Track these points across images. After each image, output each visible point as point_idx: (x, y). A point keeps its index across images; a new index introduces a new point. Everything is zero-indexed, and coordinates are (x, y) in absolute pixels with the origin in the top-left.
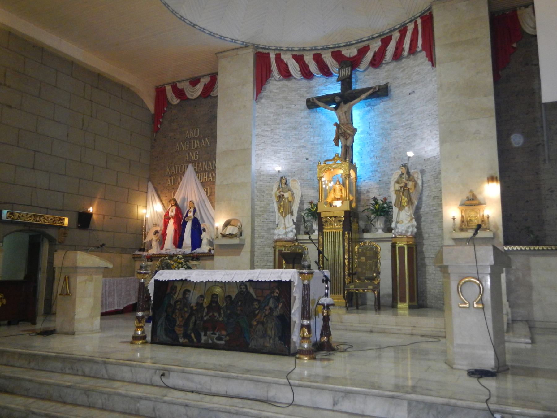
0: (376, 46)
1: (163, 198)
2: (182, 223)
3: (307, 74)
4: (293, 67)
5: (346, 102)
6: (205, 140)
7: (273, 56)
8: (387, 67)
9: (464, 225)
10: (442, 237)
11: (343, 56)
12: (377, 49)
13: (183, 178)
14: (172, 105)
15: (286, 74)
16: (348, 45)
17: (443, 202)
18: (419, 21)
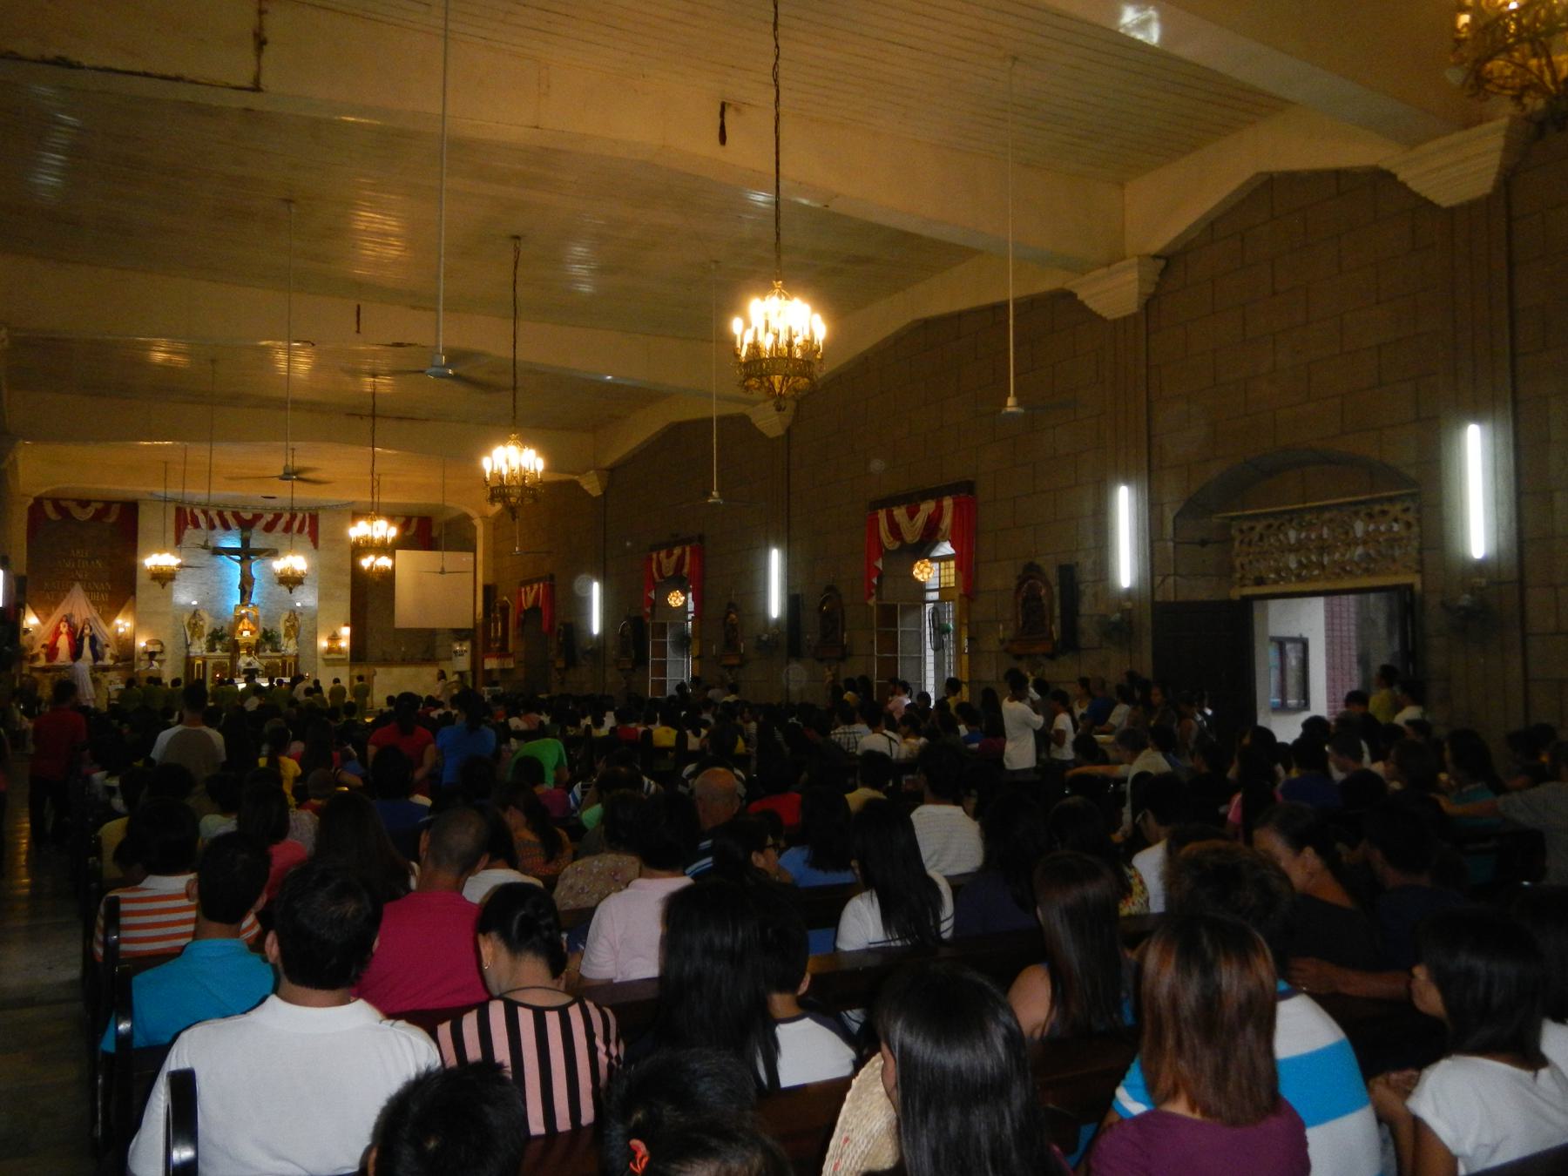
0: (269, 517)
1: (39, 612)
2: (78, 637)
3: (212, 527)
4: (202, 518)
5: (249, 558)
6: (95, 562)
7: (188, 510)
8: (277, 534)
9: (330, 651)
10: (316, 657)
11: (240, 517)
12: (269, 519)
13: (68, 596)
14: (49, 519)
15: (197, 525)
16: (244, 508)
17: (318, 636)
18: (307, 515)
